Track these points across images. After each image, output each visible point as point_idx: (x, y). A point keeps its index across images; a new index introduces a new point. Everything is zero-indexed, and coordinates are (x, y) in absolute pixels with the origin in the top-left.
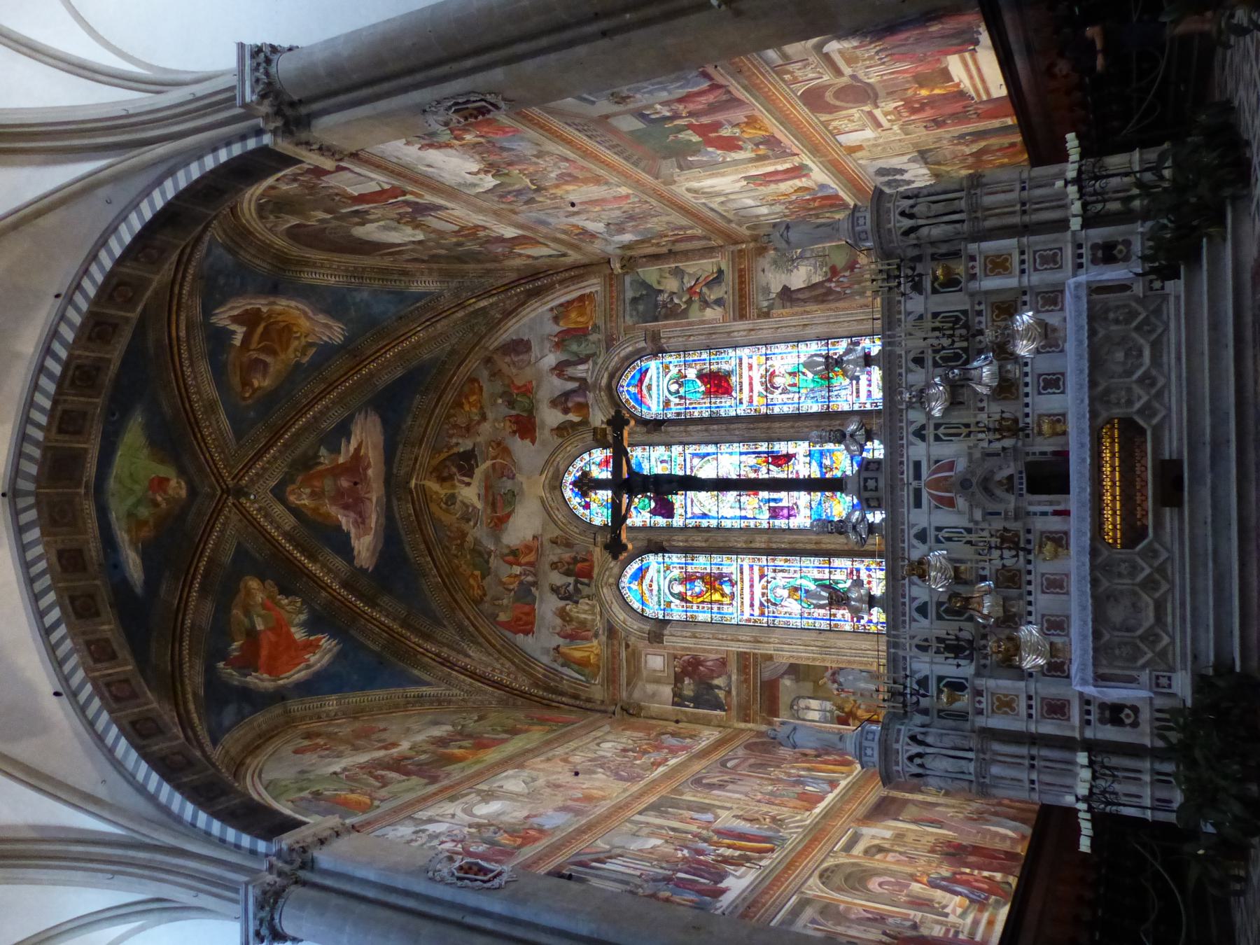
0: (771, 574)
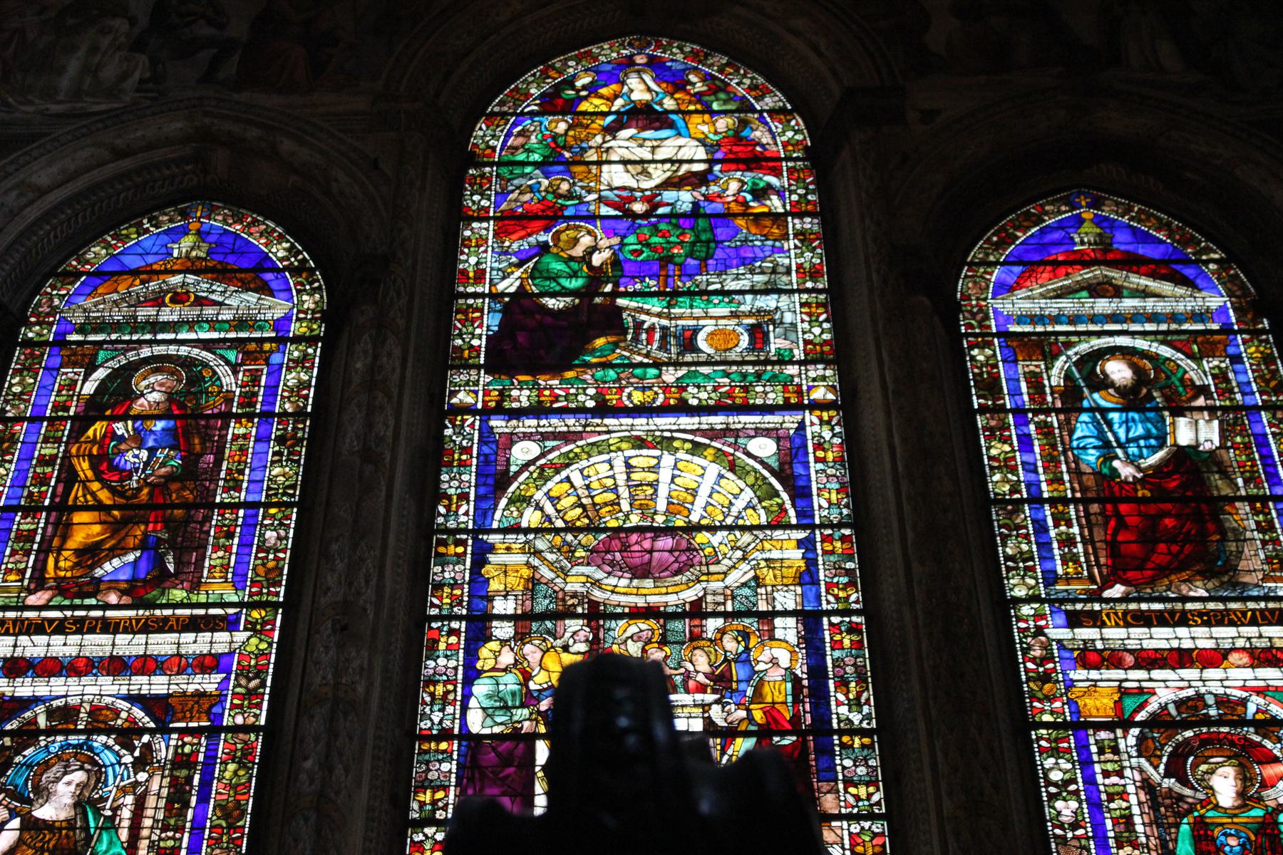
0: (164, 750)
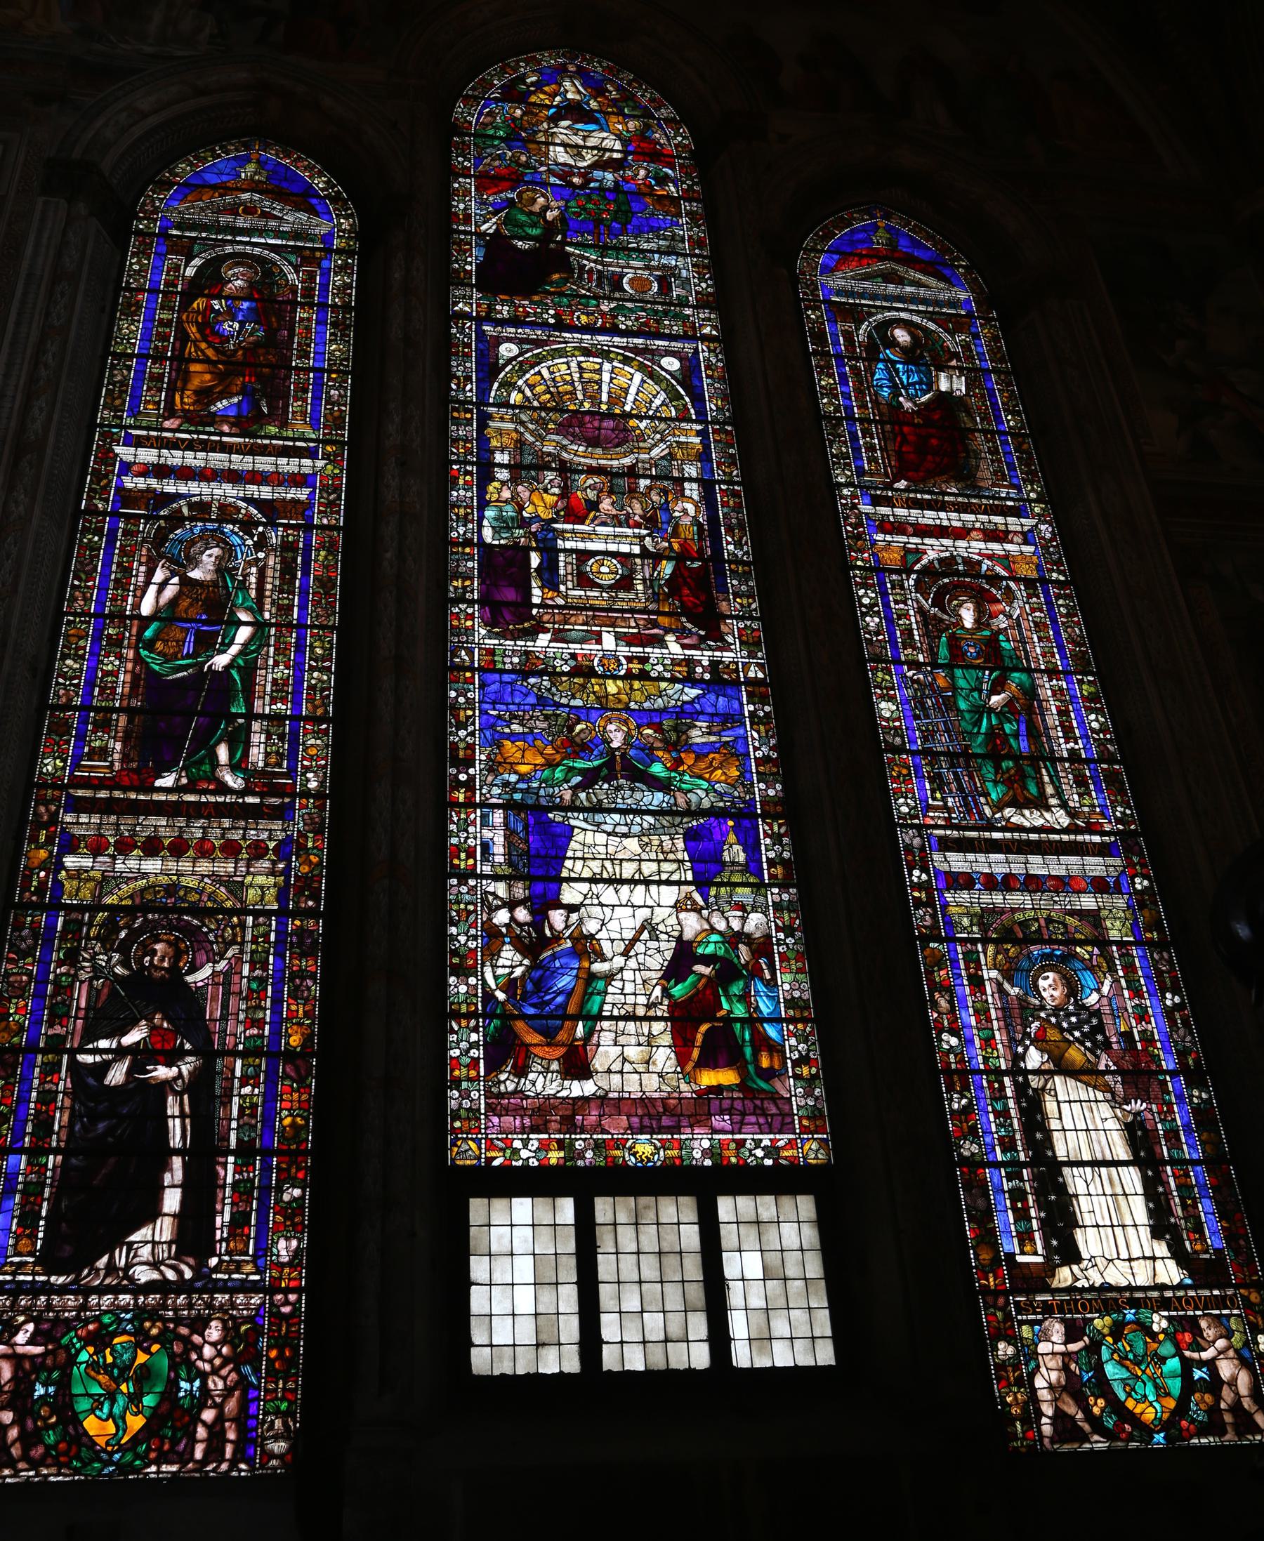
0: (274, 538)
